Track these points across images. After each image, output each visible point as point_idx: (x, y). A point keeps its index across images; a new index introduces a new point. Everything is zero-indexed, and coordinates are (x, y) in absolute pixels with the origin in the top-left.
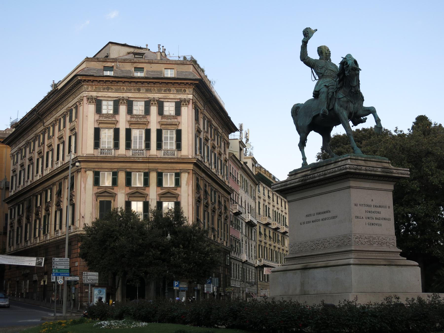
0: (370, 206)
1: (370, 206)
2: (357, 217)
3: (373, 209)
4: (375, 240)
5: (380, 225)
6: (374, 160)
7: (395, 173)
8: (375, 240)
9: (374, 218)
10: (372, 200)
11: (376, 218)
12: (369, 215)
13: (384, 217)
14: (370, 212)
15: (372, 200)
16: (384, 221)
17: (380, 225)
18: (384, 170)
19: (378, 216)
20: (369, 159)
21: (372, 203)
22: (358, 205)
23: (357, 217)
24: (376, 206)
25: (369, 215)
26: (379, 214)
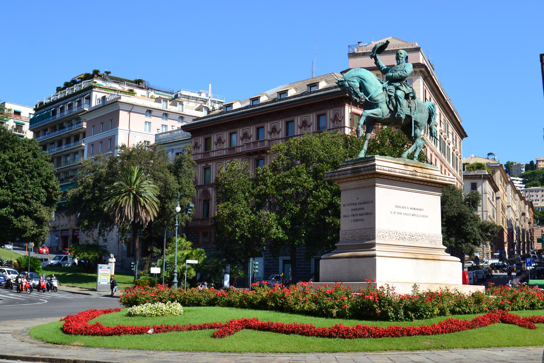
0: (356, 204)
1: (356, 204)
2: (345, 216)
3: (358, 206)
4: (357, 235)
5: (363, 220)
6: (361, 161)
7: (363, 171)
8: (357, 235)
9: (359, 215)
10: (358, 198)
11: (360, 215)
12: (355, 212)
13: (367, 212)
14: (355, 210)
15: (358, 198)
16: (367, 216)
17: (363, 220)
18: (353, 171)
19: (361, 212)
20: (357, 162)
21: (357, 201)
22: (346, 205)
23: (345, 216)
24: (360, 204)
25: (355, 212)
26: (363, 210)
